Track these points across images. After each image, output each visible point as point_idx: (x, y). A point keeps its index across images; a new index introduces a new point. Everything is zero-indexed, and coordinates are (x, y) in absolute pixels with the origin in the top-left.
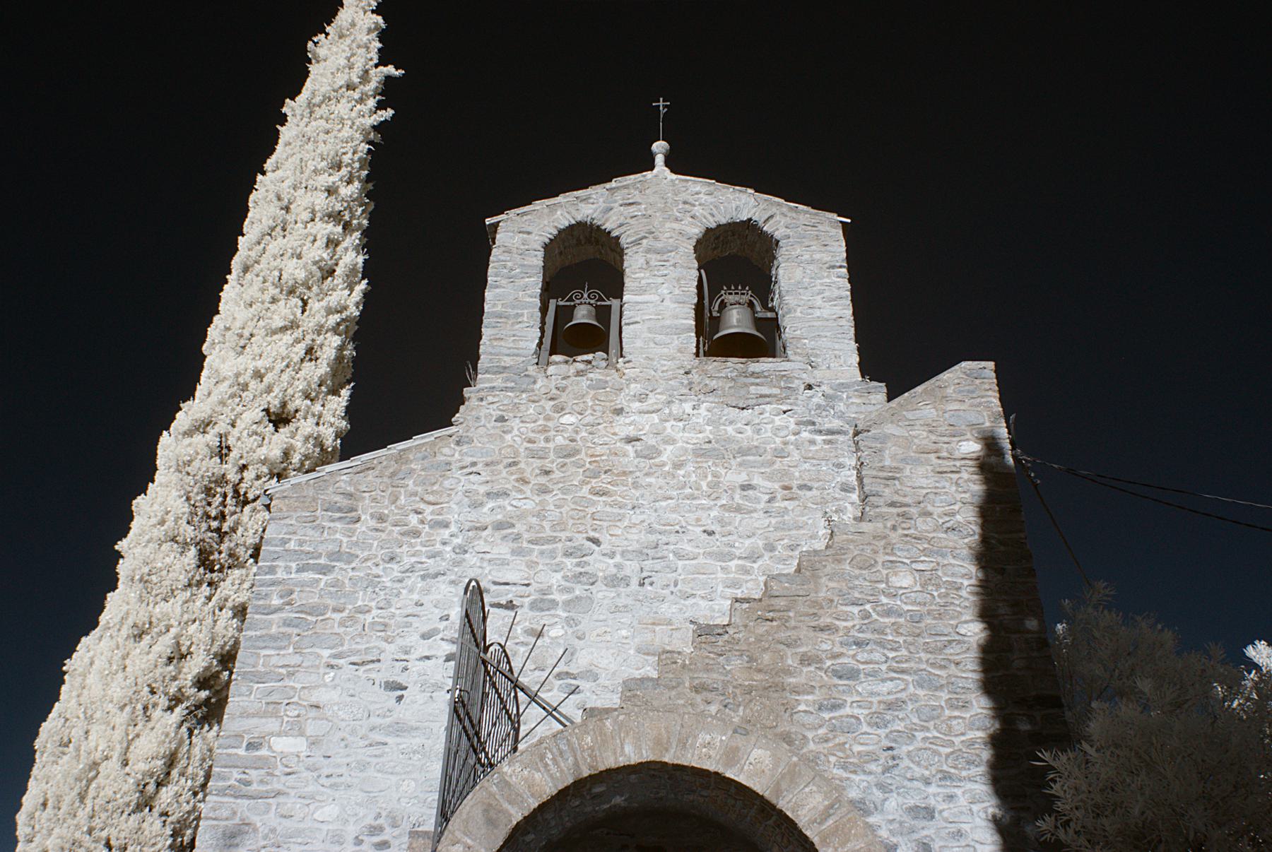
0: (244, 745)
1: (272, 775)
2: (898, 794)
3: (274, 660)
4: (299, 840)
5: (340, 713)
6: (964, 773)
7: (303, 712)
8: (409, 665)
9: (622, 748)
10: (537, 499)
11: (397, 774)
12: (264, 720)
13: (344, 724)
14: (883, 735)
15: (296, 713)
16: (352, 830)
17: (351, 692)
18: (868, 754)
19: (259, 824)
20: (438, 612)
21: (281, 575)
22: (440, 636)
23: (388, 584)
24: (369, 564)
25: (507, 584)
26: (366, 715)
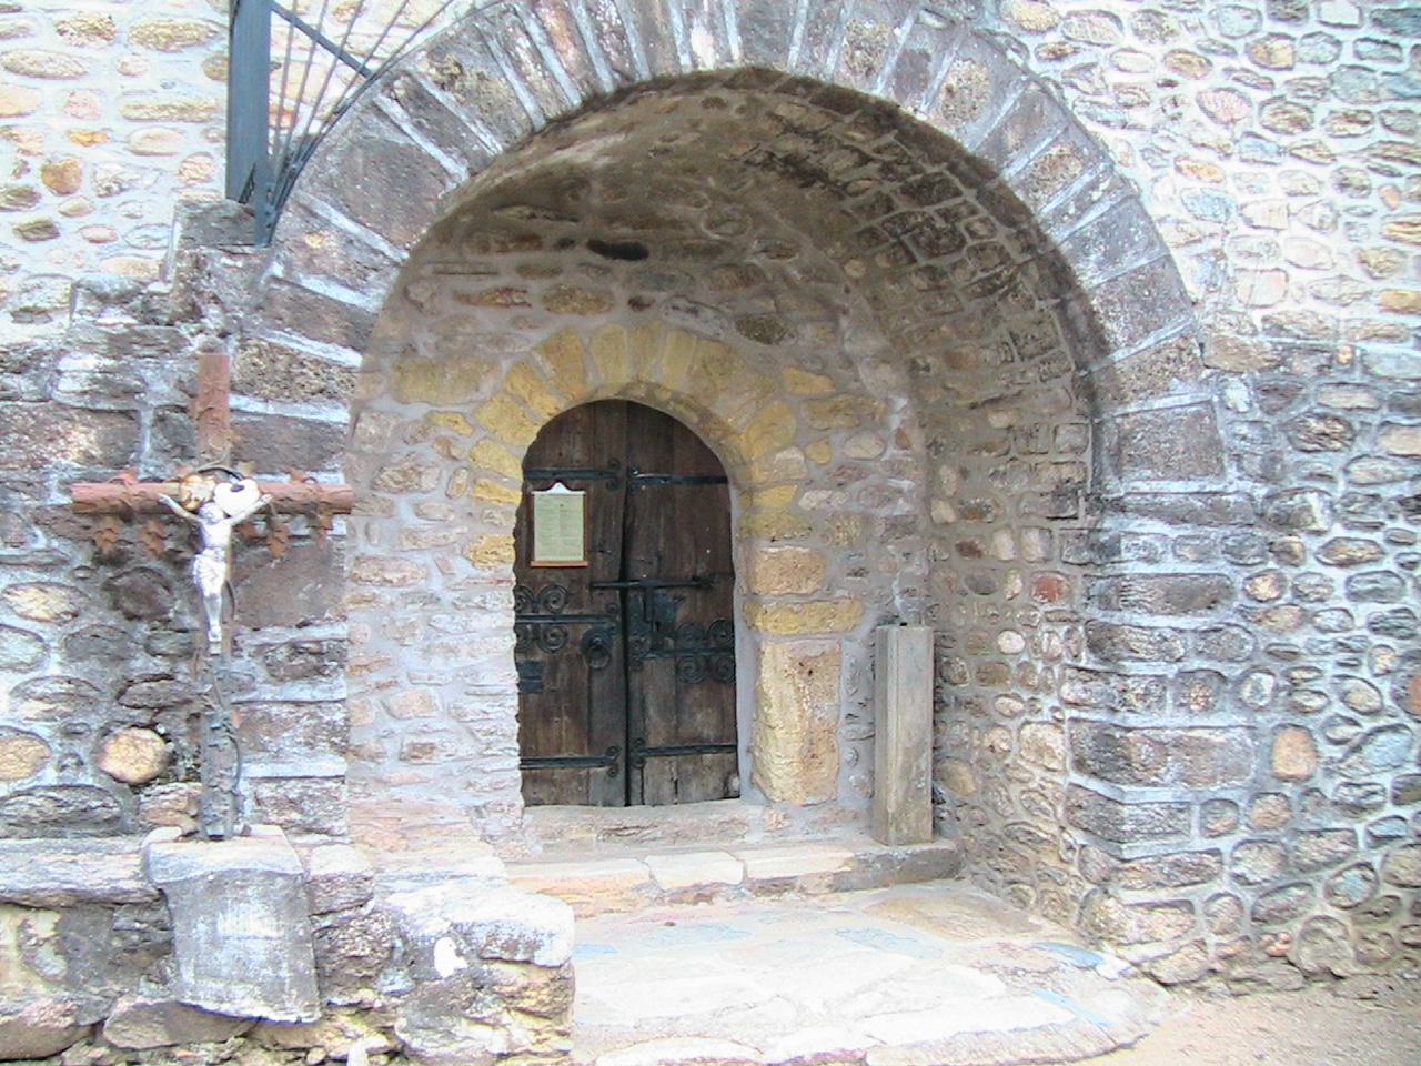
2: (1179, 170)
6: (1285, 141)
9: (688, 36)
11: (54, 77)
14: (1159, 57)
18: (1132, 90)
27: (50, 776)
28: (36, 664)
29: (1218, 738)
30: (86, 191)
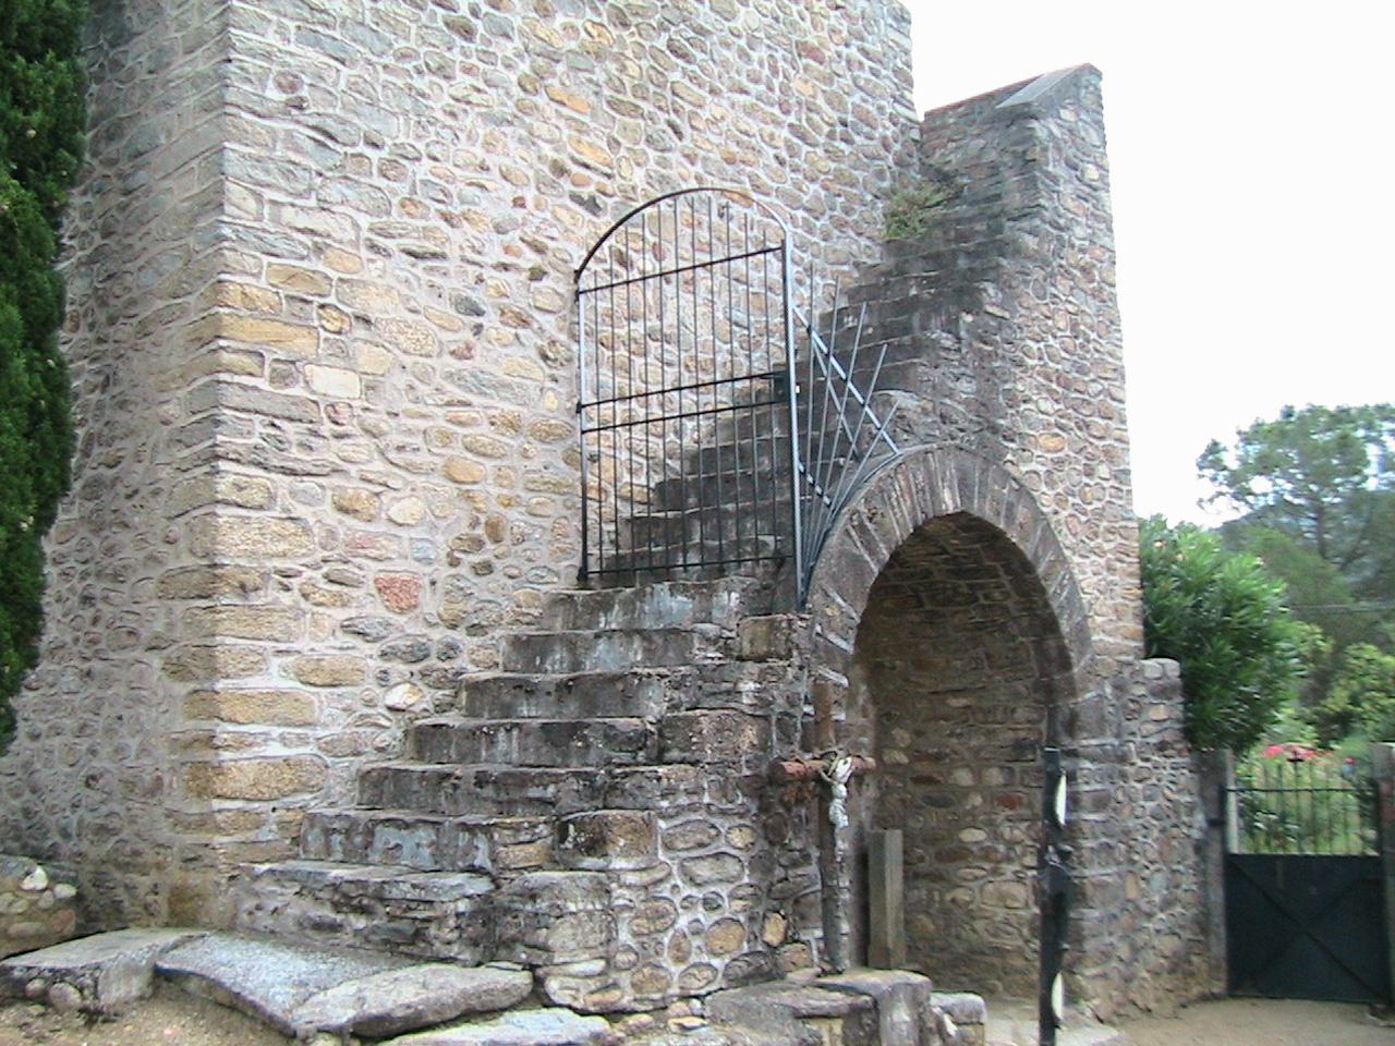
0: (267, 371)
1: (315, 434)
3: (288, 214)
4: (374, 553)
5: (402, 338)
7: (346, 327)
8: (487, 273)
10: (615, 33)
12: (289, 330)
13: (408, 360)
15: (335, 326)
16: (442, 543)
17: (413, 304)
19: (311, 520)
20: (508, 191)
21: (272, 39)
22: (517, 234)
23: (440, 115)
24: (409, 66)
25: (587, 166)
26: (436, 349)
27: (746, 947)
28: (739, 877)
29: (1109, 879)
30: (507, 541)
